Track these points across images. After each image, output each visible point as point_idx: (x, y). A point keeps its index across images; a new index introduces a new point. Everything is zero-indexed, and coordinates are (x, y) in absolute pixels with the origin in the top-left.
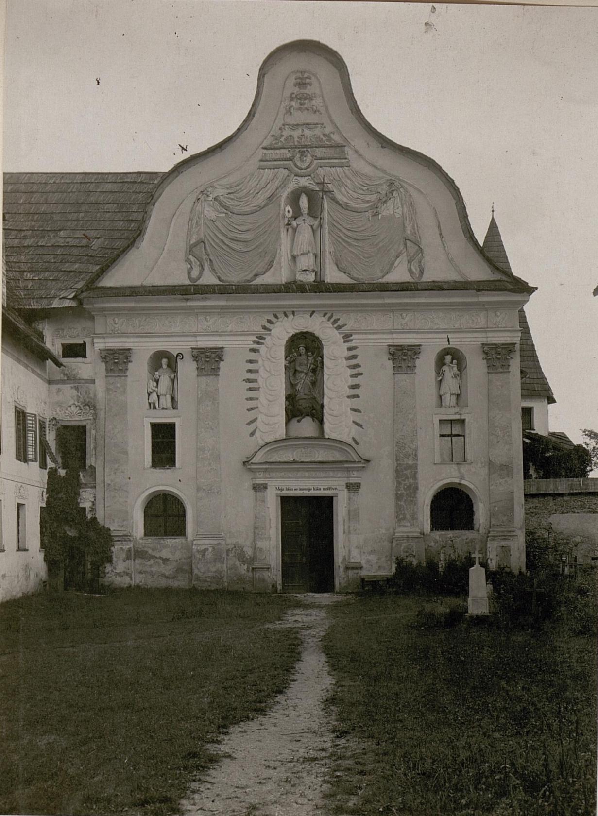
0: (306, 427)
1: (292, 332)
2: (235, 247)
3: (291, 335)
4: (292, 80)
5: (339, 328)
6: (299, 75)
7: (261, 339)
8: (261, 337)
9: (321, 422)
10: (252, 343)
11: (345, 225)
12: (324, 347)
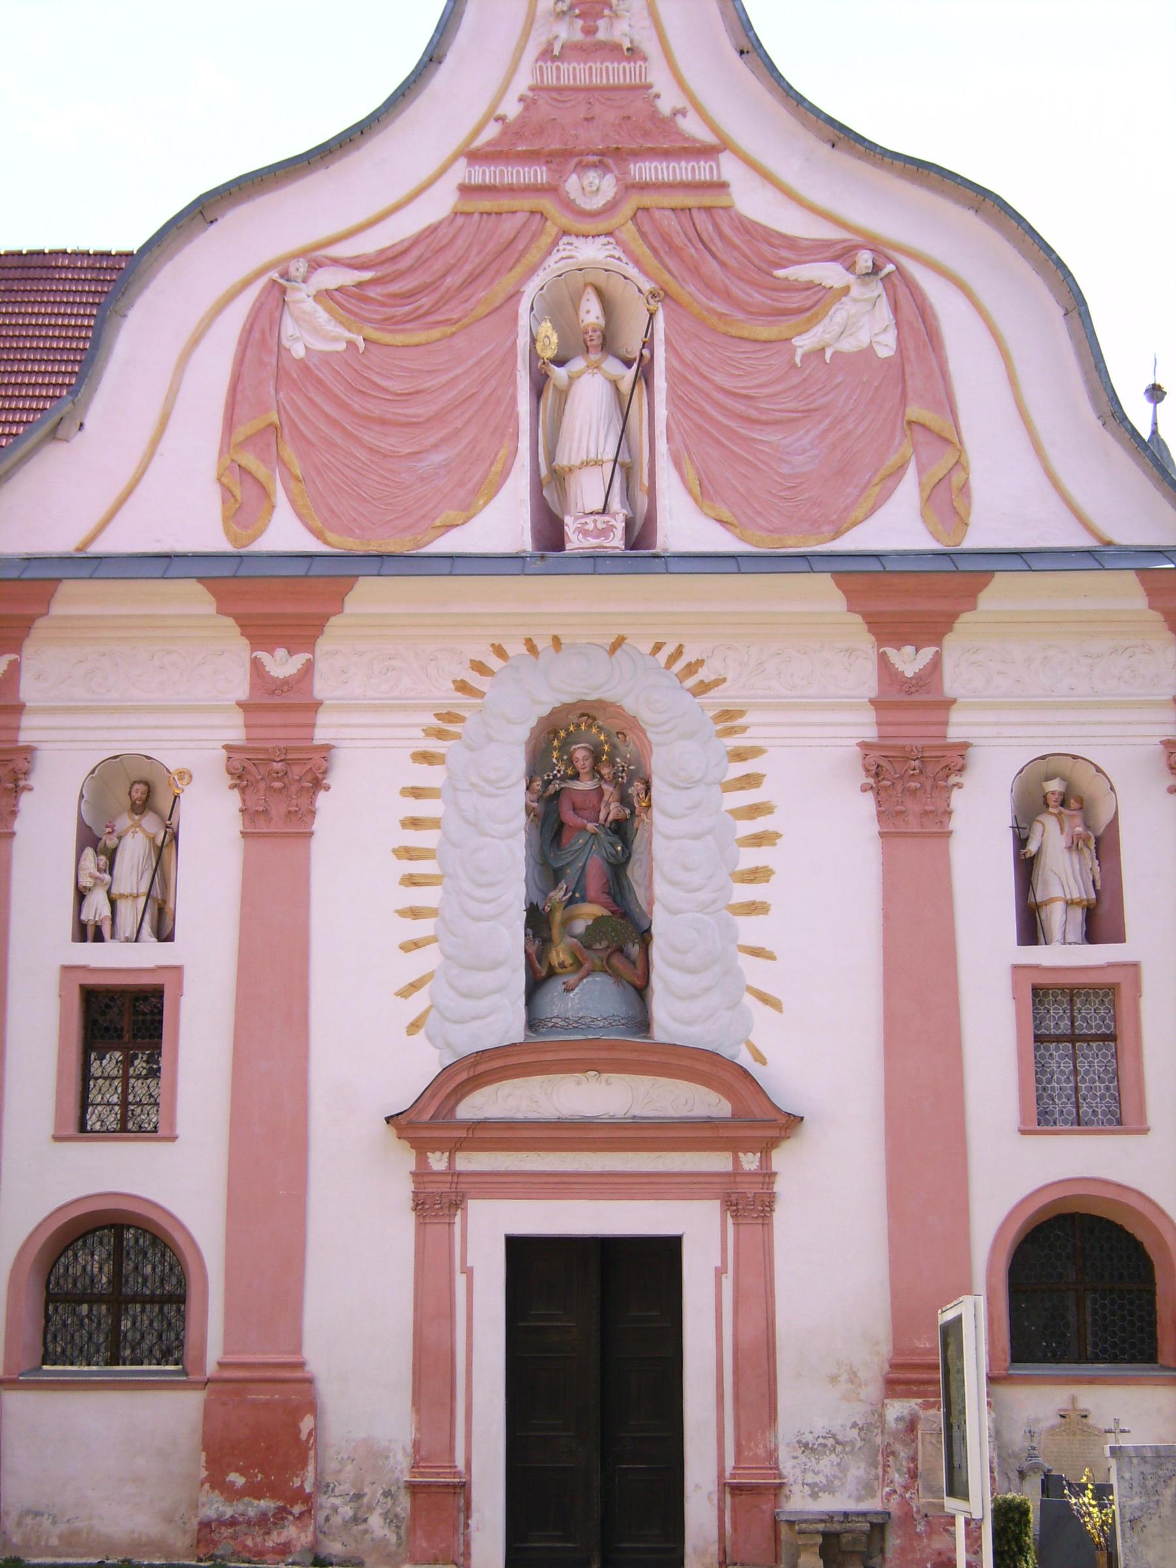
2: (383, 444)
3: (545, 711)
5: (703, 688)
7: (450, 721)
8: (451, 717)
9: (641, 990)
10: (423, 734)
11: (720, 379)
12: (655, 749)
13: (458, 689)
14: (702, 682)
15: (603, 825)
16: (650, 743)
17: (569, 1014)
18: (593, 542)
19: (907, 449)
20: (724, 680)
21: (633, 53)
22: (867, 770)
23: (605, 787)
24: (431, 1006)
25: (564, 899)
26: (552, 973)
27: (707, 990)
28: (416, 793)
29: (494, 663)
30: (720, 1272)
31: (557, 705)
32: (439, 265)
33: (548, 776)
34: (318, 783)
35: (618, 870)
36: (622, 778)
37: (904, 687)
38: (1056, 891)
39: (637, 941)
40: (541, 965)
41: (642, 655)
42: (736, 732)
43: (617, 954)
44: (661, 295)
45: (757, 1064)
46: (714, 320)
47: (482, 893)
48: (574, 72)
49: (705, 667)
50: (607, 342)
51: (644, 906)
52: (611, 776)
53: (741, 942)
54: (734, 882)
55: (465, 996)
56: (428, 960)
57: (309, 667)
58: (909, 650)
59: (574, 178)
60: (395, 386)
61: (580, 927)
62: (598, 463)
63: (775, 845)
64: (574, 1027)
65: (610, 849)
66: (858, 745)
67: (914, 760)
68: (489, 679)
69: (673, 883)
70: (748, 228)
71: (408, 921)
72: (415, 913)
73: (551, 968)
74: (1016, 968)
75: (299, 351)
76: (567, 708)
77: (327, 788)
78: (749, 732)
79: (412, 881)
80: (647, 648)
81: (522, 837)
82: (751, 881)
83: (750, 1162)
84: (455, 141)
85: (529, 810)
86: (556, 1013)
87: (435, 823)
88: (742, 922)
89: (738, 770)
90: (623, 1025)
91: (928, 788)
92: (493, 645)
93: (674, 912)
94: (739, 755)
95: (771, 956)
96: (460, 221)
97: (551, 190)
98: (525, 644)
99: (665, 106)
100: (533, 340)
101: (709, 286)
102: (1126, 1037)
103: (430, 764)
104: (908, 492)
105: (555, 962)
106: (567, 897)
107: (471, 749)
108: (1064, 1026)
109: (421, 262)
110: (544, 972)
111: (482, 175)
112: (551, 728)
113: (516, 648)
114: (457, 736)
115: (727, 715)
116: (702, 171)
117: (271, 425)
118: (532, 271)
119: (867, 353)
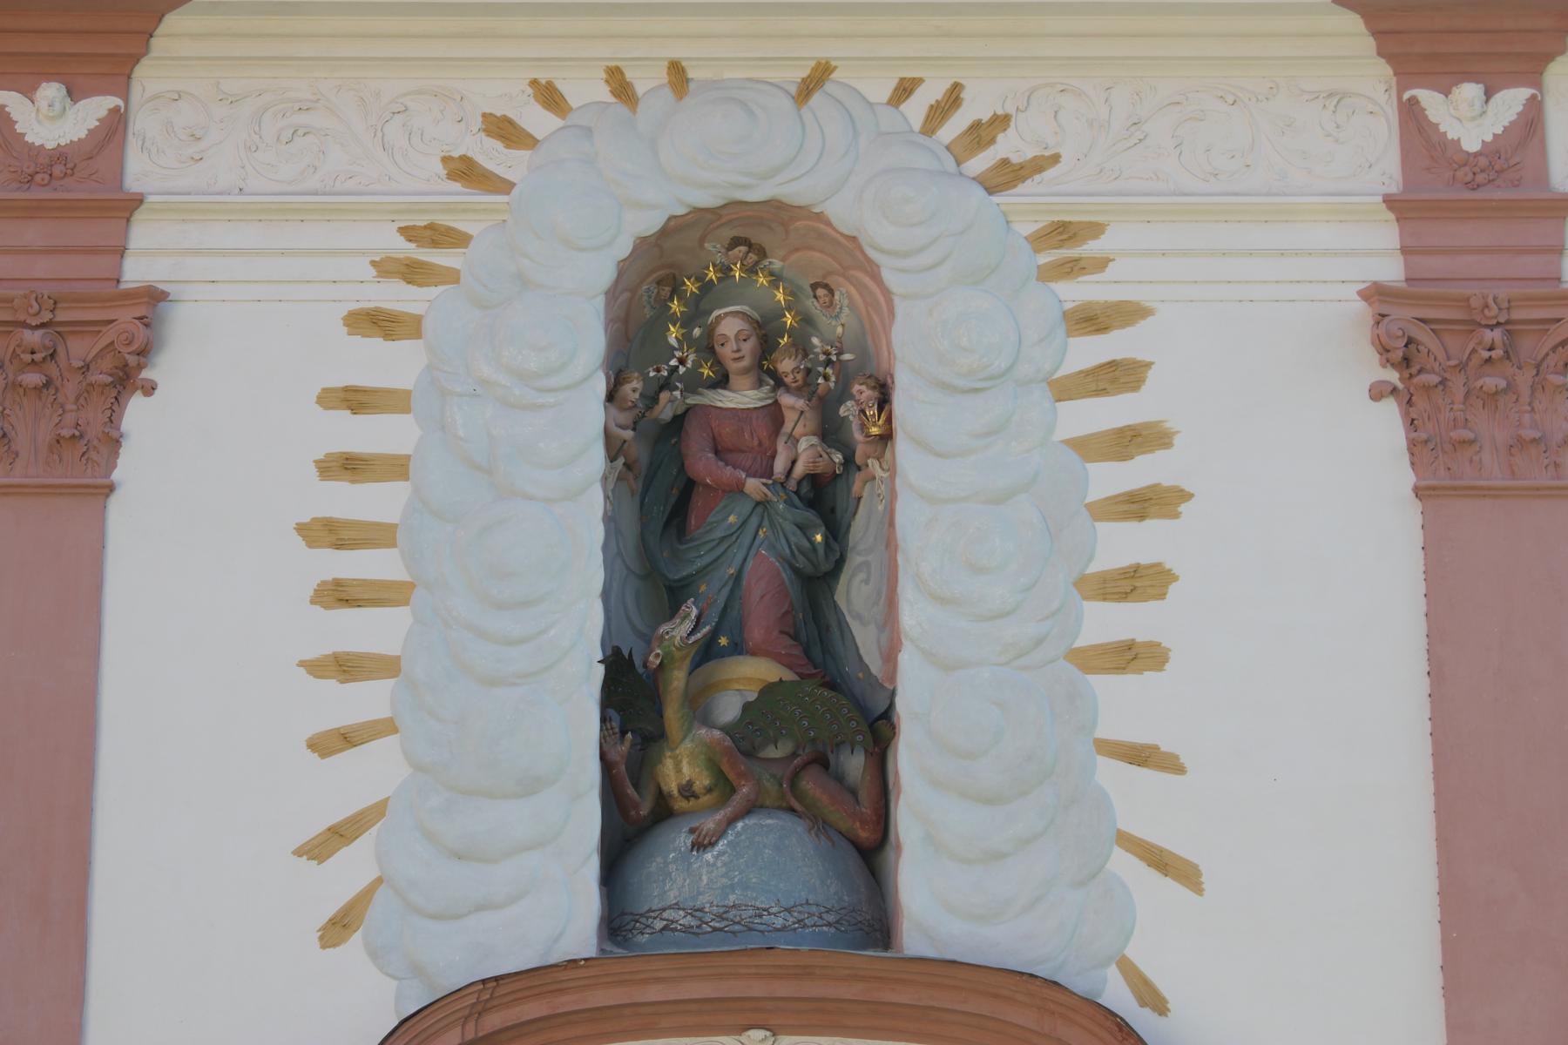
3: (651, 223)
5: (1005, 177)
7: (435, 244)
12: (900, 307)
13: (452, 176)
14: (1005, 162)
15: (782, 484)
16: (887, 293)
17: (703, 900)
20: (1055, 159)
22: (1384, 350)
23: (787, 400)
24: (379, 881)
25: (693, 639)
26: (663, 812)
28: (355, 400)
29: (537, 120)
31: (681, 211)
33: (658, 370)
36: (826, 378)
37: (1460, 174)
39: (859, 738)
40: (636, 786)
41: (871, 105)
42: (1083, 270)
43: (815, 770)
45: (1147, 1012)
49: (1011, 131)
51: (875, 665)
52: (799, 377)
53: (1105, 731)
54: (1086, 598)
57: (114, 129)
58: (1470, 92)
61: (729, 708)
63: (1176, 515)
64: (715, 929)
65: (797, 538)
66: (1360, 293)
67: (1491, 327)
68: (524, 154)
72: (346, 667)
73: (662, 798)
76: (700, 221)
77: (150, 389)
78: (1111, 272)
79: (339, 595)
80: (881, 91)
81: (595, 502)
82: (1124, 596)
85: (614, 448)
86: (672, 897)
87: (395, 468)
88: (1104, 685)
89: (1089, 351)
90: (829, 924)
91: (1525, 391)
92: (534, 83)
94: (1090, 320)
98: (607, 81)
103: (388, 335)
105: (672, 785)
106: (699, 635)
112: (667, 271)
113: (586, 90)
114: (451, 277)
115: (1062, 232)
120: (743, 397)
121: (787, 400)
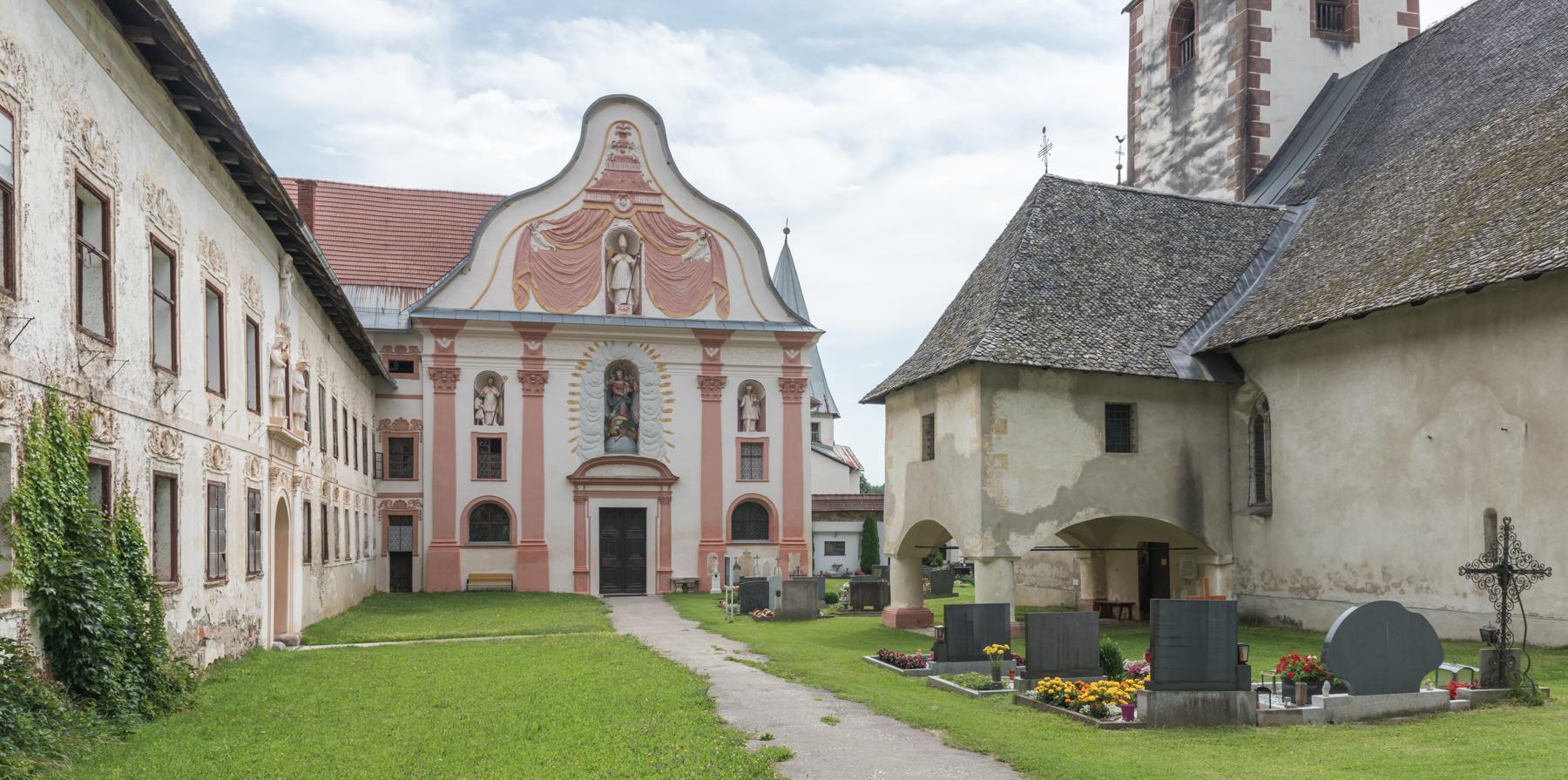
0: (622, 444)
1: (611, 359)
2: (561, 280)
3: (609, 362)
4: (614, 129)
5: (655, 357)
6: (620, 125)
9: (636, 441)
18: (623, 313)
19: (713, 290)
21: (635, 161)
26: (611, 435)
27: (654, 442)
28: (573, 385)
30: (657, 517)
32: (578, 224)
34: (545, 381)
35: (629, 406)
38: (749, 417)
44: (645, 239)
46: (659, 248)
47: (593, 414)
48: (619, 166)
50: (628, 251)
55: (588, 442)
56: (577, 432)
59: (618, 200)
60: (564, 262)
62: (625, 289)
69: (646, 413)
70: (669, 219)
71: (572, 422)
72: (573, 419)
74: (737, 438)
75: (536, 250)
79: (572, 410)
83: (665, 489)
84: (583, 185)
87: (578, 394)
88: (664, 423)
89: (663, 381)
93: (646, 420)
94: (664, 377)
95: (671, 433)
96: (584, 211)
97: (611, 203)
99: (645, 179)
100: (606, 251)
101: (658, 237)
102: (764, 457)
104: (713, 303)
107: (588, 372)
108: (749, 453)
109: (572, 223)
110: (609, 435)
111: (591, 197)
116: (654, 200)
117: (528, 273)
118: (606, 228)
119: (702, 260)
120: (621, 382)
121: (627, 383)
